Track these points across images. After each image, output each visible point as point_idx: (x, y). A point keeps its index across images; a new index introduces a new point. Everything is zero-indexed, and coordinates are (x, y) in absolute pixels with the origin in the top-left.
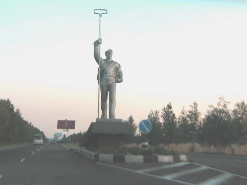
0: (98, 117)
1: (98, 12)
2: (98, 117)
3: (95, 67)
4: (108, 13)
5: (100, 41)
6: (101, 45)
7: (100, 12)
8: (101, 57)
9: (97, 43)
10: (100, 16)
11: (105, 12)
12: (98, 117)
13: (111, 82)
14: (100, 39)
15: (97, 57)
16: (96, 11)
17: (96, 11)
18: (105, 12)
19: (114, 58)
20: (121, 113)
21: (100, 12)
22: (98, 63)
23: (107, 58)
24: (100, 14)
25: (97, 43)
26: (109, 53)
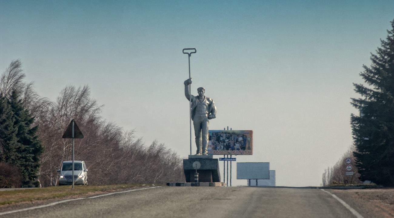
0: (228, 162)
1: (187, 52)
2: (228, 162)
3: (187, 105)
4: (197, 51)
5: (189, 81)
6: (191, 84)
7: (189, 51)
8: (192, 95)
9: (188, 83)
10: (190, 55)
11: (194, 51)
12: (190, 155)
13: (203, 119)
14: (190, 79)
15: (188, 95)
16: (185, 51)
17: (185, 51)
18: (194, 51)
19: (206, 94)
20: (192, 155)
21: (189, 51)
22: (189, 99)
23: (199, 95)
24: (189, 53)
25: (188, 83)
26: (200, 90)
